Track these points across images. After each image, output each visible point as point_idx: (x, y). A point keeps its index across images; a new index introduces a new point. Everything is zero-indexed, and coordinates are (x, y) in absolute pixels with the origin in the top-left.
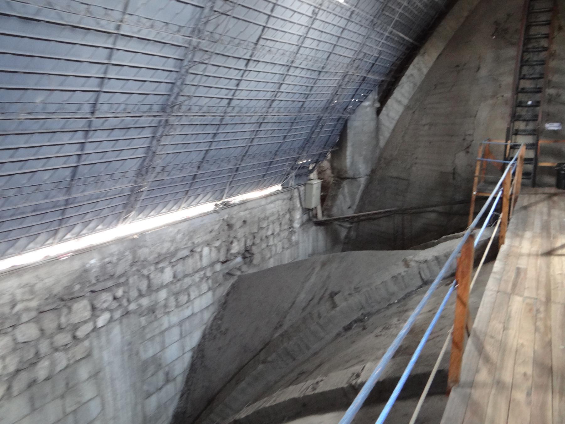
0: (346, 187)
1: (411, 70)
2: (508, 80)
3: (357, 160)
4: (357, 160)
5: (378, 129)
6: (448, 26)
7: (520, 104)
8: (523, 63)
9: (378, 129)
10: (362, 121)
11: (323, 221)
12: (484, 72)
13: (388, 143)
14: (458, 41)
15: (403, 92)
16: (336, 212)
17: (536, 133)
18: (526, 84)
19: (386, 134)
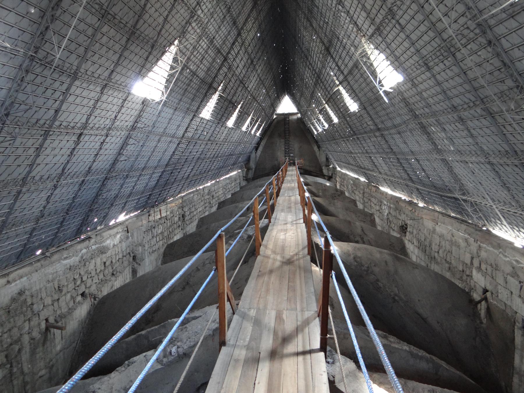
0: (250, 171)
1: (262, 143)
2: (283, 146)
3: (252, 165)
4: (252, 165)
5: (256, 157)
6: (268, 133)
7: (286, 151)
8: (285, 143)
9: (256, 157)
10: (253, 156)
11: (247, 179)
12: (278, 144)
13: (259, 160)
14: (271, 137)
15: (261, 149)
16: (248, 177)
17: (289, 156)
18: (287, 147)
19: (258, 158)
